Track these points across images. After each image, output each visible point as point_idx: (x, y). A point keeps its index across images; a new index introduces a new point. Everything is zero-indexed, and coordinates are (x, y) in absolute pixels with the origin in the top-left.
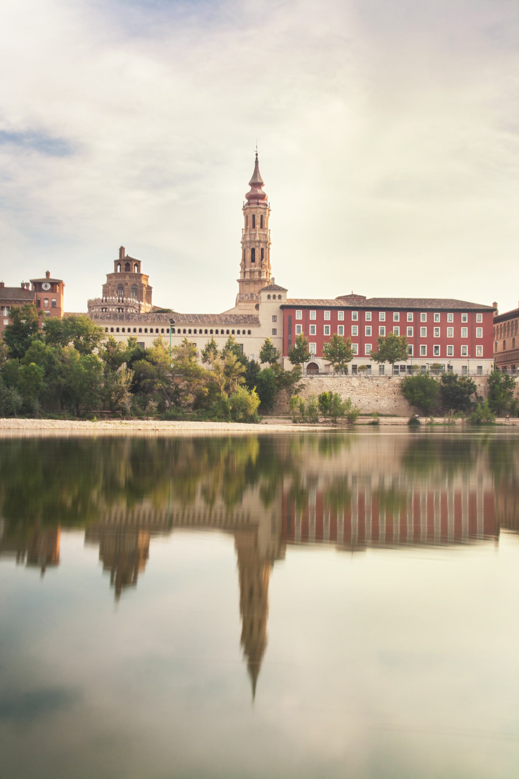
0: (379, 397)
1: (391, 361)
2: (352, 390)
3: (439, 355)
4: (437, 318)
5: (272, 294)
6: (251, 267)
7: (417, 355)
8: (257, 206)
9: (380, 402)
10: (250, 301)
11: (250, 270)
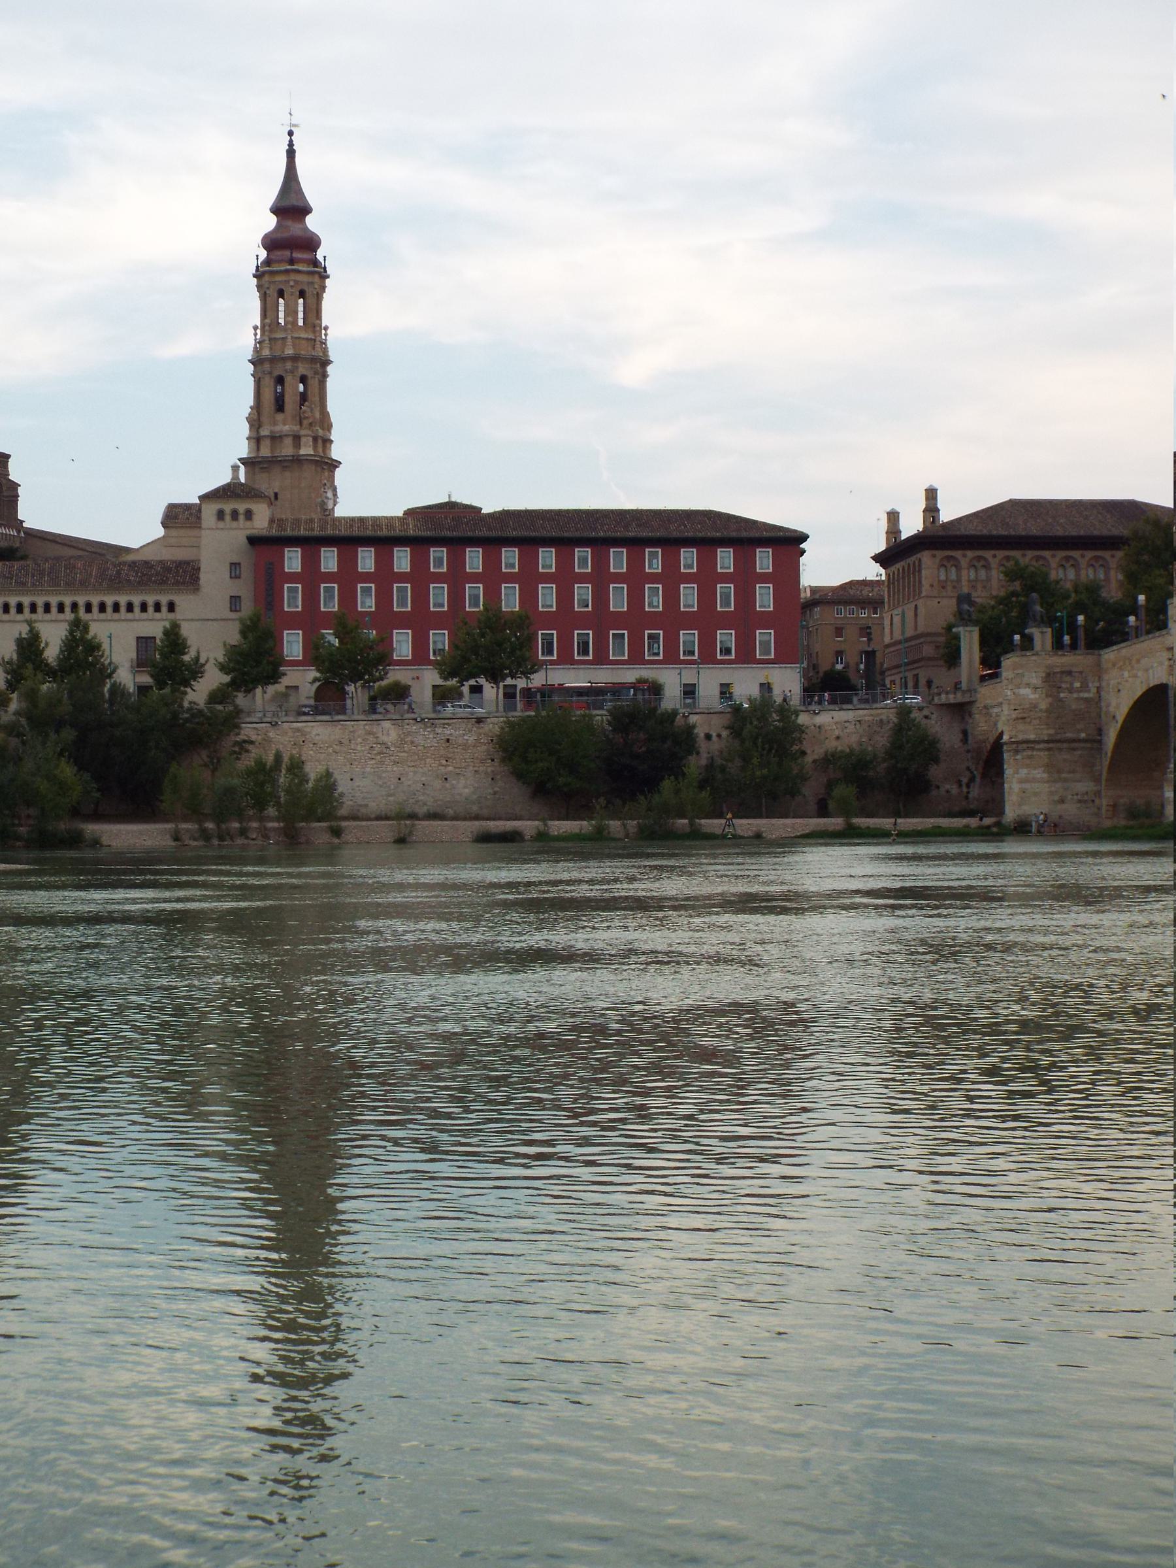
0: (450, 768)
1: (495, 678)
3: (661, 657)
4: (655, 561)
5: (228, 507)
6: (275, 423)
7: (566, 659)
9: (454, 782)
11: (271, 432)
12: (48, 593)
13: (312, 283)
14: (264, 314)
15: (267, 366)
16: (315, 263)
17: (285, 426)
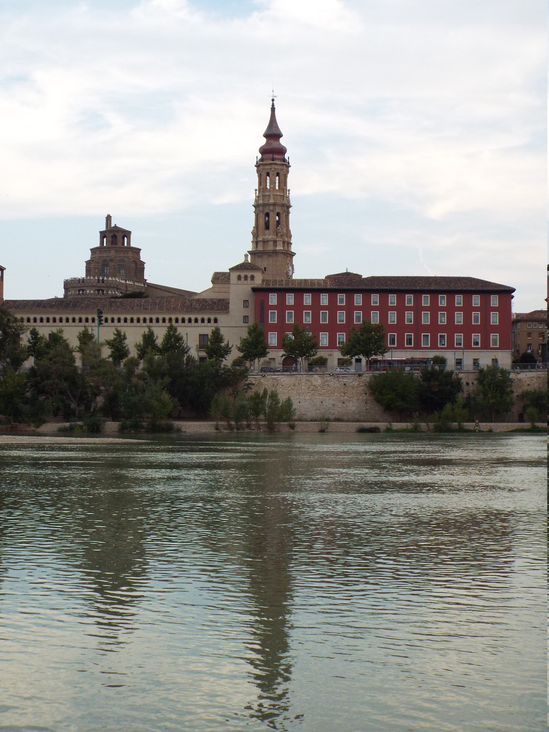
0: (346, 398)
1: (367, 354)
2: (313, 390)
3: (446, 346)
4: (443, 301)
5: (243, 274)
6: (265, 235)
7: (401, 346)
8: (272, 162)
9: (348, 404)
10: (225, 281)
11: (263, 239)
12: (158, 313)
13: (283, 169)
14: (260, 184)
15: (261, 208)
16: (284, 160)
17: (269, 236)
